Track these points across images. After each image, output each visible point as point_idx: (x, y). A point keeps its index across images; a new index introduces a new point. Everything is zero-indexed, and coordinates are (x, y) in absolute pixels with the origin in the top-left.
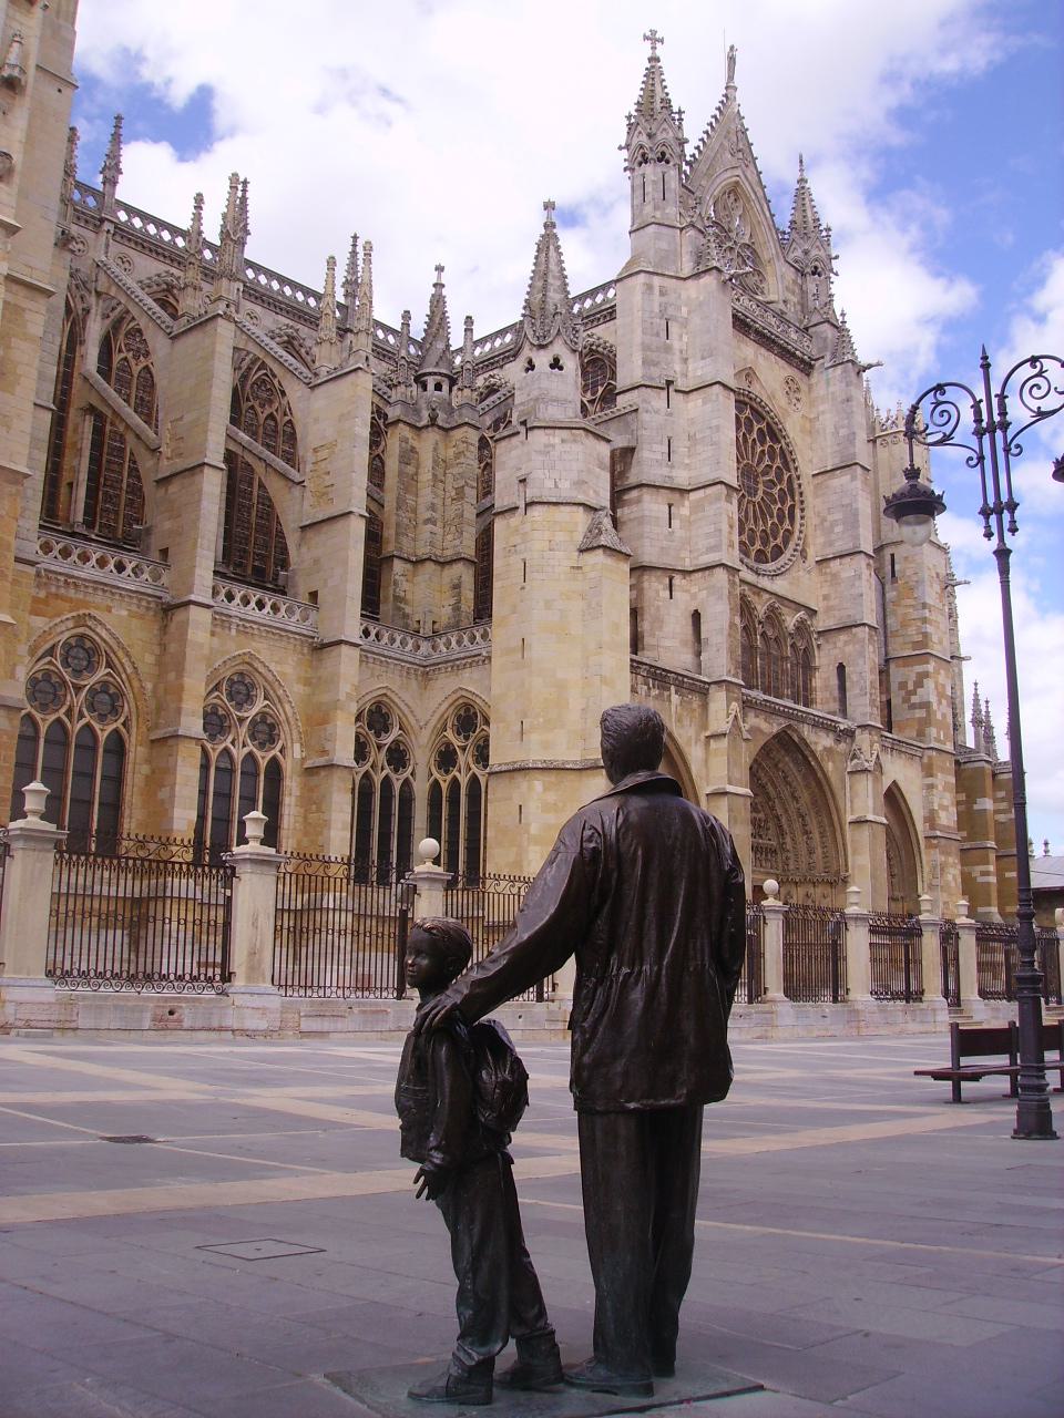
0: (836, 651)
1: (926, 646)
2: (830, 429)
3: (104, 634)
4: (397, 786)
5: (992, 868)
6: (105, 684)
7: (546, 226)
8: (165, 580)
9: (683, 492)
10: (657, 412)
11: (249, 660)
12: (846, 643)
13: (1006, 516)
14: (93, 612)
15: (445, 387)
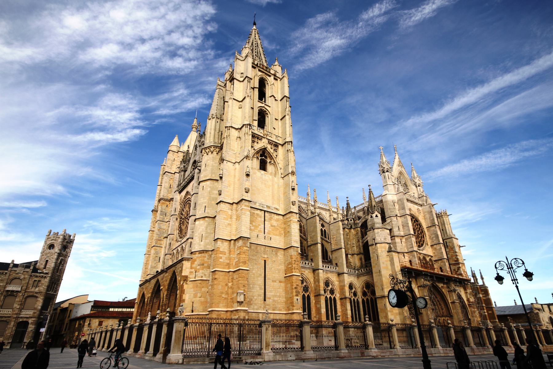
0: (439, 265)
1: (458, 261)
2: (428, 218)
3: (305, 276)
4: (356, 300)
5: (485, 311)
6: (305, 286)
7: (369, 190)
8: (313, 265)
9: (403, 236)
10: (395, 221)
11: (328, 278)
12: (441, 263)
13: (516, 281)
14: (303, 272)
15: (352, 220)
